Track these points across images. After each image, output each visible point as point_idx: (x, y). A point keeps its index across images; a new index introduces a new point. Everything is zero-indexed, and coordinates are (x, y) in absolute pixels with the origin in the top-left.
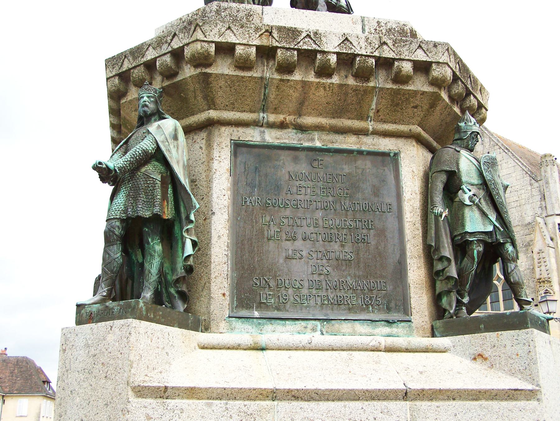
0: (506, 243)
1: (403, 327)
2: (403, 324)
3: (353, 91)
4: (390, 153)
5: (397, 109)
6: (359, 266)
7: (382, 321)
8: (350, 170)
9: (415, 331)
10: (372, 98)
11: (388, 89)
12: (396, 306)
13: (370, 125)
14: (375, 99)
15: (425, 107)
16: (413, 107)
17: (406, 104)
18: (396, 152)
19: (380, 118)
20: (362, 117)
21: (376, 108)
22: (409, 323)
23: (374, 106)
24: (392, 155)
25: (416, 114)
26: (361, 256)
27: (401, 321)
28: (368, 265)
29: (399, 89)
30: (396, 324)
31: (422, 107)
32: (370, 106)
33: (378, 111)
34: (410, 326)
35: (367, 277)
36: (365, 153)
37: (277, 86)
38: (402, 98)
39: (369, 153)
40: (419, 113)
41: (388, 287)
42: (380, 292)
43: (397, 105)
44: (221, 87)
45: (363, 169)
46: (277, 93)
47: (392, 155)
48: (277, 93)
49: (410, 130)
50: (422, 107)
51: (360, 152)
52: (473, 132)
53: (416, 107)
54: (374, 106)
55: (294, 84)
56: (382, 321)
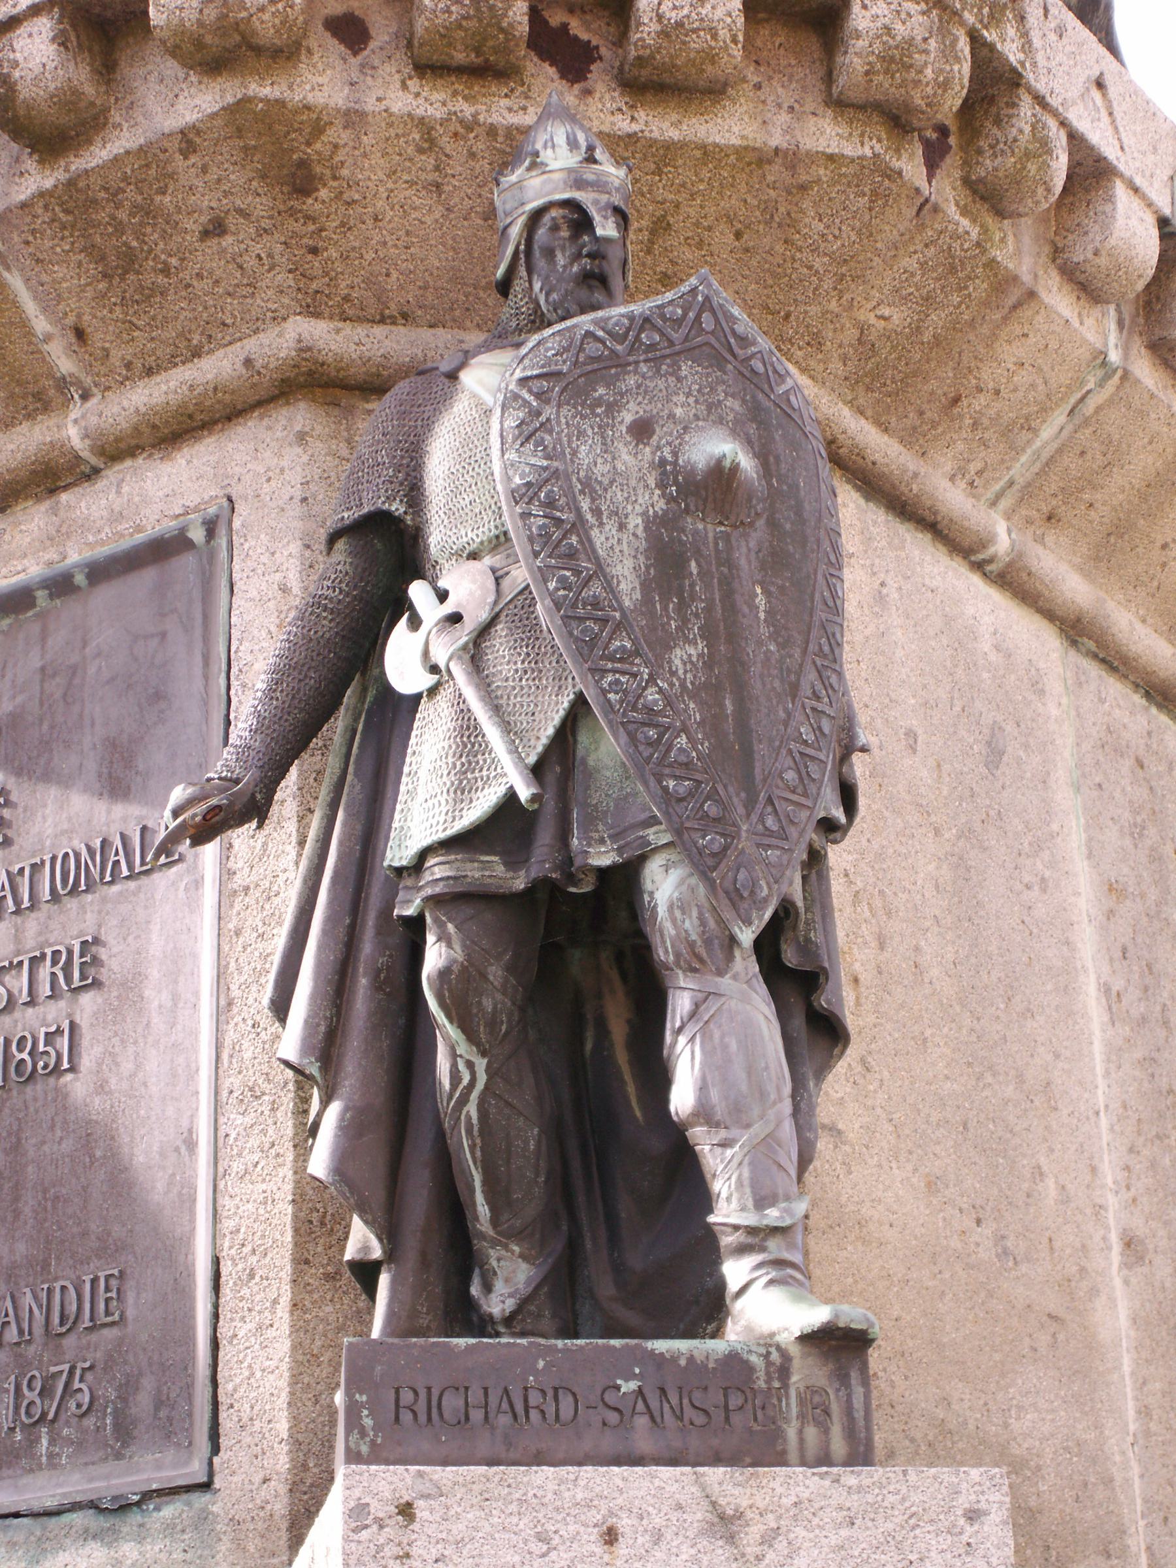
0: (643, 859)
1: (170, 1529)
2: (170, 1510)
4: (183, 530)
5: (149, 278)
6: (17, 1213)
7: (75, 1507)
8: (19, 699)
9: (224, 1547)
11: (24, 205)
12: (159, 1404)
13: (73, 429)
16: (206, 234)
17: (164, 235)
18: (212, 510)
20: (41, 396)
22: (200, 1500)
24: (197, 535)
25: (250, 262)
26: (31, 1153)
27: (160, 1493)
28: (57, 1198)
29: (71, 183)
30: (135, 1517)
34: (204, 1517)
35: (46, 1265)
38: (122, 215)
39: (100, 572)
41: (130, 1297)
42: (94, 1337)
43: (130, 261)
45: (74, 670)
47: (197, 535)
49: (248, 362)
50: (243, 213)
51: (61, 585)
52: (536, 216)
56: (75, 1507)
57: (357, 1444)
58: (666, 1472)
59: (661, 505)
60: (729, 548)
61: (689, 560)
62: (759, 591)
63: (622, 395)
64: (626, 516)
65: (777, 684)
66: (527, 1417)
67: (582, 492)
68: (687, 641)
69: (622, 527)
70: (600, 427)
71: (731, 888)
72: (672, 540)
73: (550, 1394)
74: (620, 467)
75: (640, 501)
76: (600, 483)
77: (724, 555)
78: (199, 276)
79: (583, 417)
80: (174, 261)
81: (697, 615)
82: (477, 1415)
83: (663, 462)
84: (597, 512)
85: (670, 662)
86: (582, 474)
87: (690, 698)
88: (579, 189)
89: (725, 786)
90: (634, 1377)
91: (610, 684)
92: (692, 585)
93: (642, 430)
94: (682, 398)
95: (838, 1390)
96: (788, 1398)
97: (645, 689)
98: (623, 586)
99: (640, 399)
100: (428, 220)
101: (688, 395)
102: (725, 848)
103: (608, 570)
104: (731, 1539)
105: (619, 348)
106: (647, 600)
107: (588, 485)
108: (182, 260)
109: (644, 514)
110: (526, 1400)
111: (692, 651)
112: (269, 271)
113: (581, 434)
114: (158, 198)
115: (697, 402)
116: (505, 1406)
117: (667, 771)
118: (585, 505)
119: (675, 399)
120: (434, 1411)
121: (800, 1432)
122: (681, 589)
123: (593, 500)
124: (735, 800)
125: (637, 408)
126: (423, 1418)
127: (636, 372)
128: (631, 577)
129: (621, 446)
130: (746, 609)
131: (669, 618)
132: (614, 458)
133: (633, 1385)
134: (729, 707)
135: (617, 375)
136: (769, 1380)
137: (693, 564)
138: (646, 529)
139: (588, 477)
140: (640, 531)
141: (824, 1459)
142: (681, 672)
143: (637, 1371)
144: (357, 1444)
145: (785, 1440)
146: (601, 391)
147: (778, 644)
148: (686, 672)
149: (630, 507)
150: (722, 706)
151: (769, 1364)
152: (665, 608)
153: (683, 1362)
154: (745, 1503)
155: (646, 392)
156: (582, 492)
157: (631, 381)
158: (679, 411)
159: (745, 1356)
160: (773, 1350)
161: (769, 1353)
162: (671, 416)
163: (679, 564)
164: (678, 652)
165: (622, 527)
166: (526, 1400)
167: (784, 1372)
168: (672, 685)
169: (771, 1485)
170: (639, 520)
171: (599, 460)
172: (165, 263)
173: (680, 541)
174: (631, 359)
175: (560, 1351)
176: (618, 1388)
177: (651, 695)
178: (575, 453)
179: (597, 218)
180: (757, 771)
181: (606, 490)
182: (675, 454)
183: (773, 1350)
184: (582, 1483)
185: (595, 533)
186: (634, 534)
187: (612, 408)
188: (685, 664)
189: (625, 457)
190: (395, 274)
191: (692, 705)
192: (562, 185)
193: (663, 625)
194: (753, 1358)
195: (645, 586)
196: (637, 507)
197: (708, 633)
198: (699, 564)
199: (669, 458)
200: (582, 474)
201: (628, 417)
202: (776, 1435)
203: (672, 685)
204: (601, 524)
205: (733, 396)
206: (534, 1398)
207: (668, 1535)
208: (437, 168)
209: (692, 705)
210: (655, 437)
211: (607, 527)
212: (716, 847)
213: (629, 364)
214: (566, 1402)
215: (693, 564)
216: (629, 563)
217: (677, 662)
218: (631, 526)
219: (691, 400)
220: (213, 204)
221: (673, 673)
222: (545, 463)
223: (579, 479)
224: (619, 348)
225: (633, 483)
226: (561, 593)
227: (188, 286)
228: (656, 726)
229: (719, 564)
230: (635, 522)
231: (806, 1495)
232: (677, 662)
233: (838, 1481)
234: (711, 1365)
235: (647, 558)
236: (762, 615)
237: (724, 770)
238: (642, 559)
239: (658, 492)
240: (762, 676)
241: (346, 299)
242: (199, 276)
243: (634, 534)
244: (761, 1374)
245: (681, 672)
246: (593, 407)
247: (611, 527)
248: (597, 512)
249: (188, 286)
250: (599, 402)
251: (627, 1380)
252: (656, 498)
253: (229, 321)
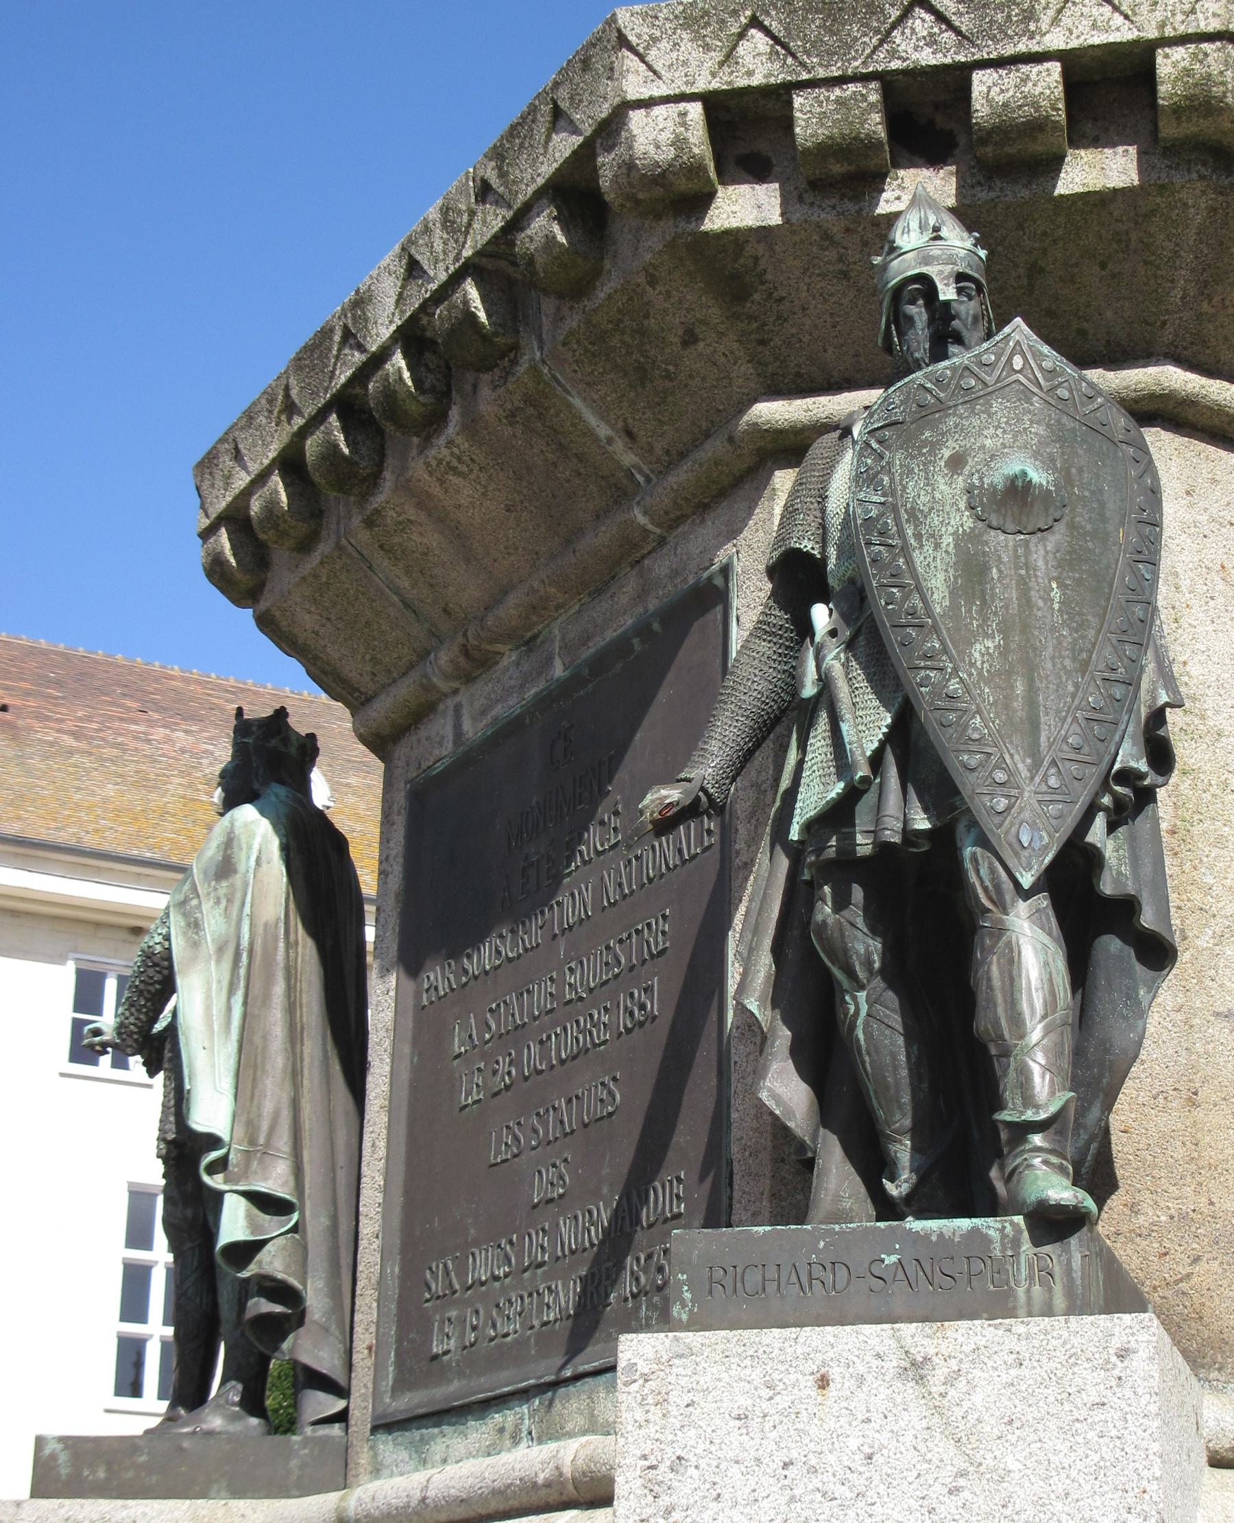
3: (511, 424)
10: (569, 406)
14: (577, 402)
15: (715, 314)
19: (658, 451)
21: (612, 427)
23: (603, 431)
31: (701, 321)
32: (596, 439)
33: (629, 434)
36: (656, 626)
37: (381, 547)
40: (721, 348)
44: (317, 633)
46: (401, 565)
48: (401, 565)
53: (690, 338)
54: (603, 431)
55: (399, 514)
57: (679, 1314)
58: (868, 1329)
59: (969, 523)
60: (1028, 552)
61: (990, 569)
62: (1054, 585)
63: (943, 434)
64: (941, 537)
65: (1067, 662)
66: (811, 1287)
67: (908, 521)
68: (987, 636)
69: (937, 546)
70: (924, 464)
71: (1014, 841)
72: (976, 553)
73: (829, 1266)
74: (938, 496)
75: (953, 523)
76: (922, 511)
77: (1023, 559)
78: (691, 376)
79: (913, 457)
80: (671, 368)
81: (996, 614)
82: (771, 1287)
83: (973, 486)
84: (918, 536)
85: (971, 655)
86: (909, 506)
87: (986, 684)
88: (926, 264)
89: (1012, 756)
90: (894, 1252)
91: (922, 679)
92: (992, 589)
93: (956, 463)
94: (992, 431)
95: (1060, 1256)
96: (1019, 1263)
97: (949, 680)
98: (935, 596)
99: (957, 436)
100: (845, 301)
101: (997, 428)
102: (1008, 808)
103: (924, 584)
104: (920, 1380)
105: (942, 395)
106: (954, 606)
107: (913, 514)
108: (676, 366)
109: (955, 533)
110: (810, 1273)
111: (990, 644)
112: (735, 364)
113: (911, 471)
114: (646, 322)
115: (1004, 432)
116: (794, 1279)
117: (963, 747)
118: (910, 532)
119: (985, 433)
120: (739, 1284)
121: (1028, 1291)
122: (983, 592)
123: (916, 526)
124: (1020, 766)
125: (954, 445)
126: (729, 1290)
127: (955, 414)
128: (943, 588)
129: (940, 479)
130: (1041, 603)
131: (972, 618)
132: (934, 489)
133: (894, 1258)
134: (1020, 688)
135: (940, 418)
136: (1004, 1249)
137: (994, 570)
138: (956, 546)
139: (913, 508)
140: (951, 549)
141: (1048, 1312)
142: (979, 663)
143: (897, 1246)
144: (679, 1314)
145: (1015, 1298)
146: (927, 434)
147: (1071, 629)
148: (983, 662)
149: (944, 529)
150: (1012, 687)
151: (1004, 1236)
152: (969, 611)
153: (934, 1238)
154: (932, 1351)
155: (962, 430)
156: (908, 521)
157: (951, 422)
158: (988, 442)
159: (984, 1231)
160: (1007, 1225)
161: (1004, 1227)
162: (983, 447)
163: (984, 570)
164: (978, 646)
165: (937, 546)
166: (810, 1273)
167: (1016, 1243)
168: (970, 675)
169: (955, 1335)
170: (951, 539)
171: (922, 493)
172: (666, 370)
173: (984, 552)
174: (951, 403)
175: (837, 1233)
176: (883, 1261)
177: (954, 685)
178: (904, 488)
179: (940, 286)
180: (1043, 739)
181: (926, 517)
182: (981, 479)
183: (1007, 1225)
184: (801, 1340)
185: (917, 557)
186: (947, 552)
187: (935, 446)
188: (983, 655)
189: (942, 487)
190: (830, 350)
191: (987, 690)
192: (913, 263)
193: (966, 625)
194: (991, 1232)
195: (953, 593)
196: (950, 528)
197: (1005, 630)
198: (1000, 571)
199: (977, 483)
200: (909, 506)
201: (947, 453)
202: (1010, 1294)
203: (970, 675)
204: (921, 546)
205: (1038, 423)
206: (817, 1270)
207: (869, 1378)
208: (840, 260)
209: (987, 690)
210: (968, 467)
211: (926, 548)
212: (1001, 808)
213: (950, 408)
214: (842, 1273)
215: (994, 570)
216: (941, 576)
217: (977, 655)
218: (944, 545)
219: (999, 432)
220: (683, 320)
221: (972, 665)
222: (883, 500)
223: (906, 510)
224: (942, 395)
225: (947, 508)
226: (890, 607)
227: (686, 386)
228: (956, 710)
229: (1017, 568)
230: (948, 540)
231: (983, 1343)
232: (977, 655)
233: (1010, 1331)
234: (957, 1239)
235: (956, 570)
236: (1056, 606)
237: (1011, 742)
238: (951, 571)
239: (967, 513)
240: (1053, 658)
241: (798, 375)
242: (691, 376)
243: (947, 552)
244: (997, 1245)
245: (979, 663)
246: (920, 448)
247: (928, 548)
248: (918, 536)
249: (686, 386)
250: (925, 443)
251: (889, 1255)
252: (965, 519)
253: (721, 408)
